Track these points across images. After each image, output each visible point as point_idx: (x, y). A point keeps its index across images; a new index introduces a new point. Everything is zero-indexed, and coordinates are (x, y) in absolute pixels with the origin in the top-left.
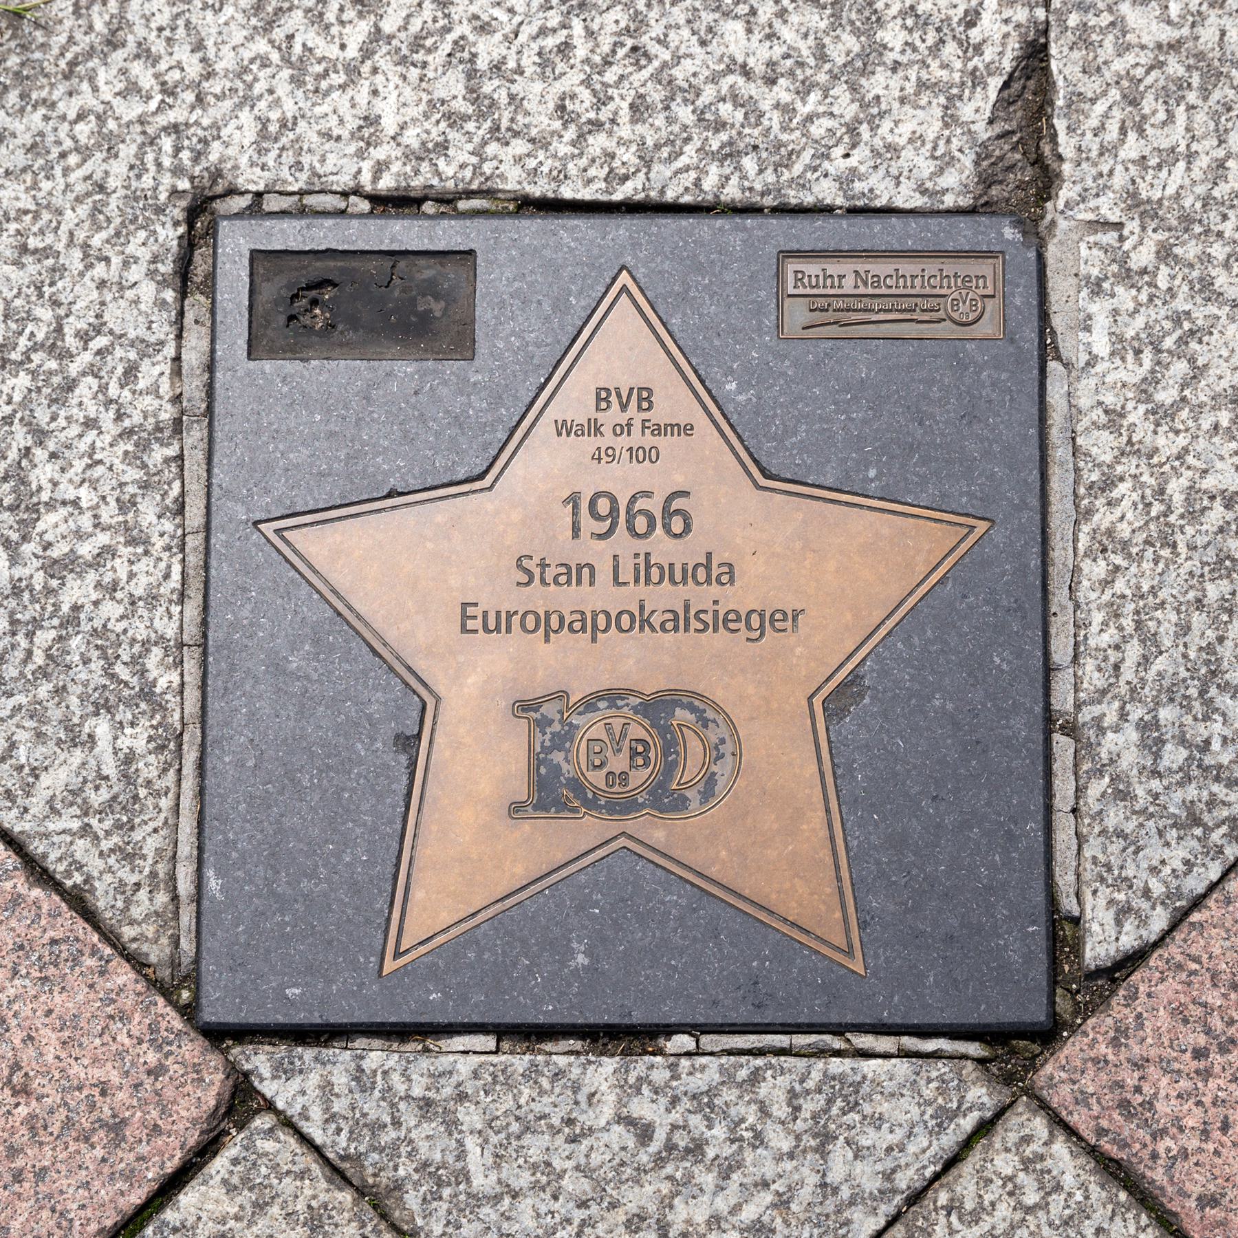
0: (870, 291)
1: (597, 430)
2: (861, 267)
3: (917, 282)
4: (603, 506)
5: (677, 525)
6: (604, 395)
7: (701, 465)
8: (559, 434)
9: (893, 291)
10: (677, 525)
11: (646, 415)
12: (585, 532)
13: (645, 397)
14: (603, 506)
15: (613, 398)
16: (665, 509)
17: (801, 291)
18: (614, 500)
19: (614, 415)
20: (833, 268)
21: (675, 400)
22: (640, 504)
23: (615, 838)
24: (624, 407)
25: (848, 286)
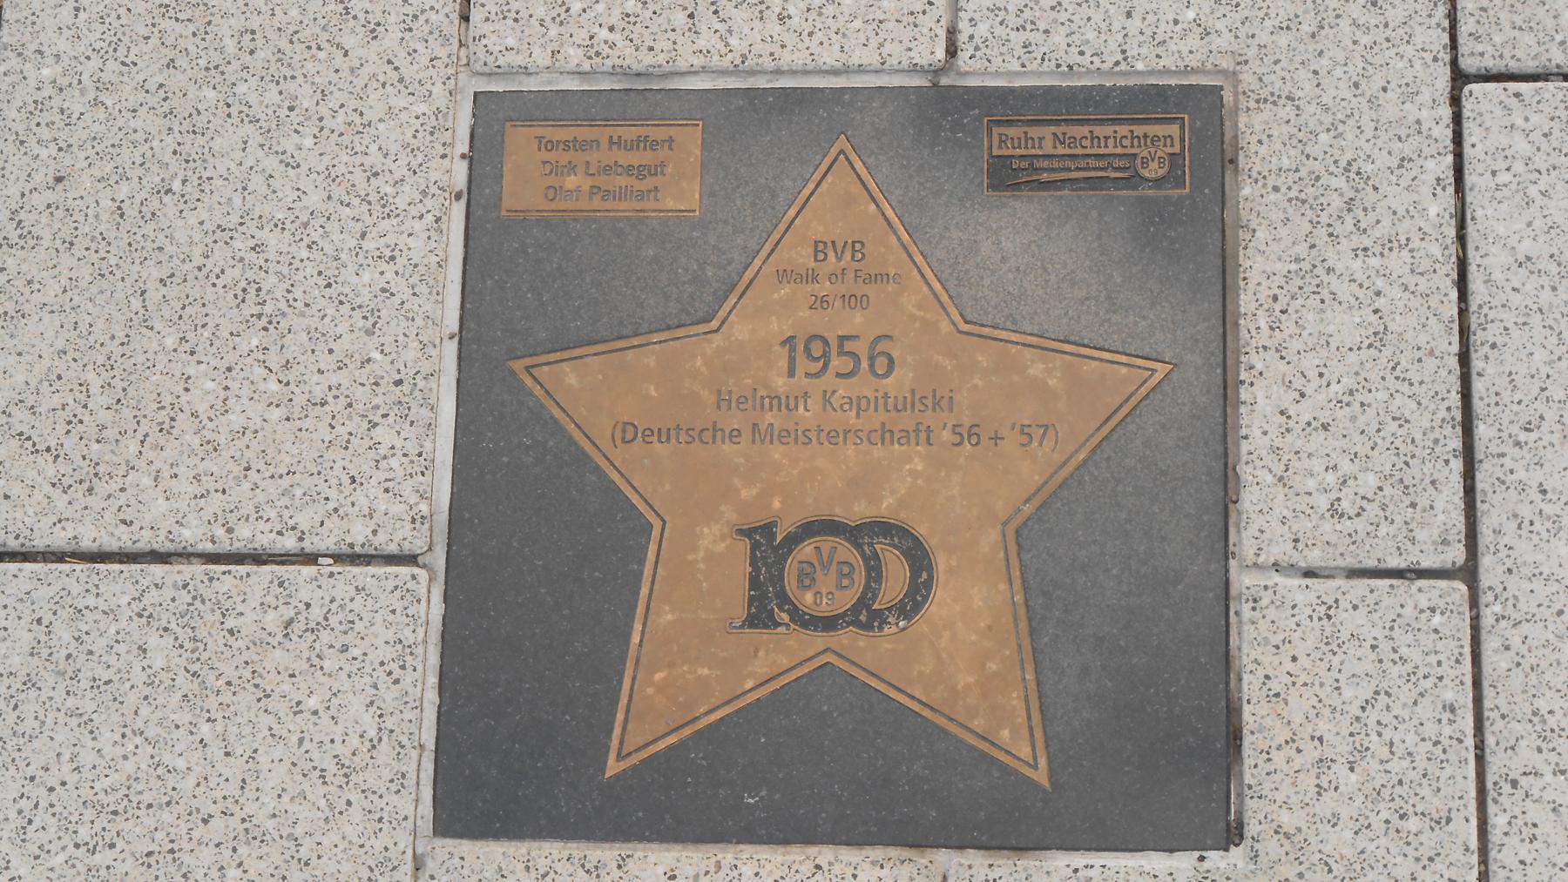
0: (1068, 151)
2: (1059, 130)
4: (817, 349)
6: (821, 246)
9: (1088, 151)
11: (856, 265)
12: (800, 371)
14: (817, 349)
16: (872, 349)
17: (1005, 152)
18: (825, 342)
20: (1035, 132)
22: (848, 346)
23: (825, 651)
24: (839, 259)
25: (1048, 148)
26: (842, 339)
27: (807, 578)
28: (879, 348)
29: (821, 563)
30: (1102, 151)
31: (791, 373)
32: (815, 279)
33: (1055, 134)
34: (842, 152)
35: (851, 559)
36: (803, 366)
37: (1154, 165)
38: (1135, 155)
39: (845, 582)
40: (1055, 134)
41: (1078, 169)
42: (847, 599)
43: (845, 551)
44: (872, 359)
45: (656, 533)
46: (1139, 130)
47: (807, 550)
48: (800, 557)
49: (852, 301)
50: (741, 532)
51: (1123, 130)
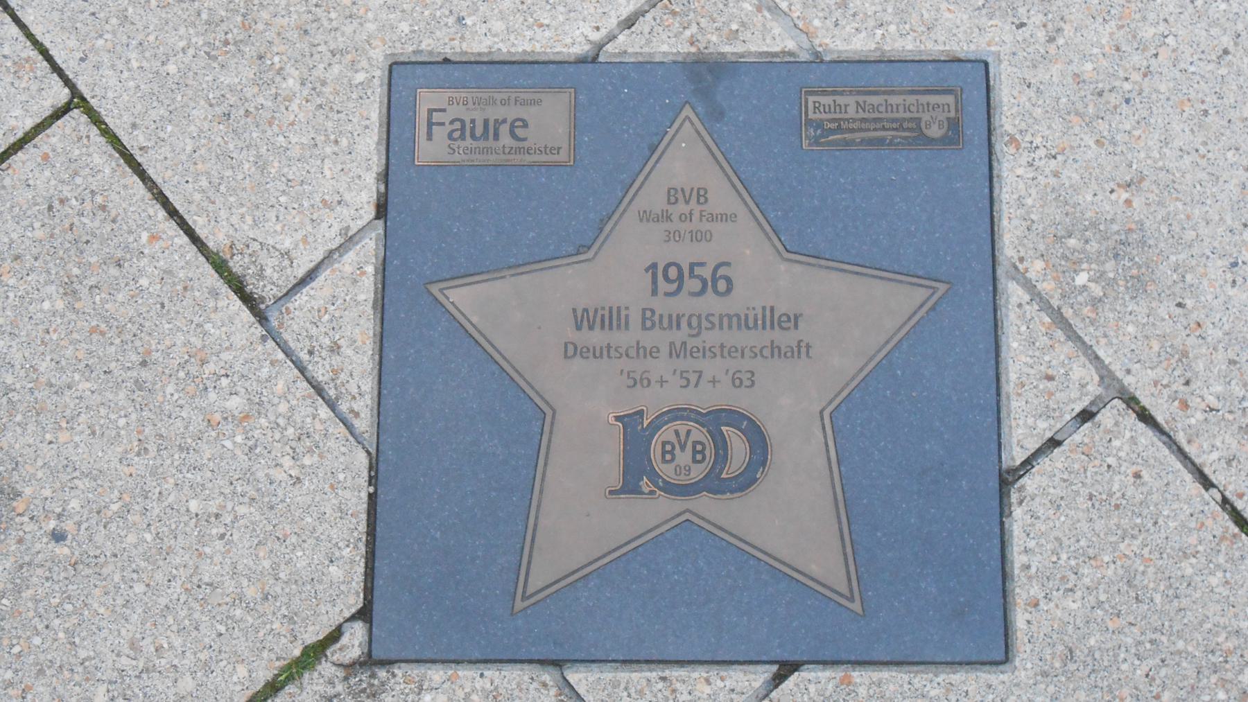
0: (866, 115)
1: (669, 218)
2: (861, 99)
3: (901, 108)
4: (673, 273)
5: (722, 285)
7: (744, 246)
8: (641, 220)
9: (883, 115)
10: (722, 285)
11: (703, 207)
13: (702, 195)
14: (673, 273)
15: (680, 196)
17: (818, 116)
19: (682, 207)
20: (841, 100)
21: (723, 196)
23: (684, 512)
24: (687, 202)
25: (851, 112)
26: (692, 266)
27: (668, 453)
28: (721, 272)
29: (679, 441)
30: (896, 115)
31: (654, 292)
32: (669, 218)
33: (858, 103)
34: (687, 118)
35: (705, 441)
36: (663, 286)
37: (935, 127)
38: (920, 119)
39: (699, 457)
40: (858, 103)
41: (875, 130)
42: (698, 472)
43: (699, 434)
44: (715, 280)
45: (548, 419)
46: (924, 99)
47: (666, 433)
48: (663, 438)
49: (698, 237)
50: (617, 418)
51: (911, 99)
